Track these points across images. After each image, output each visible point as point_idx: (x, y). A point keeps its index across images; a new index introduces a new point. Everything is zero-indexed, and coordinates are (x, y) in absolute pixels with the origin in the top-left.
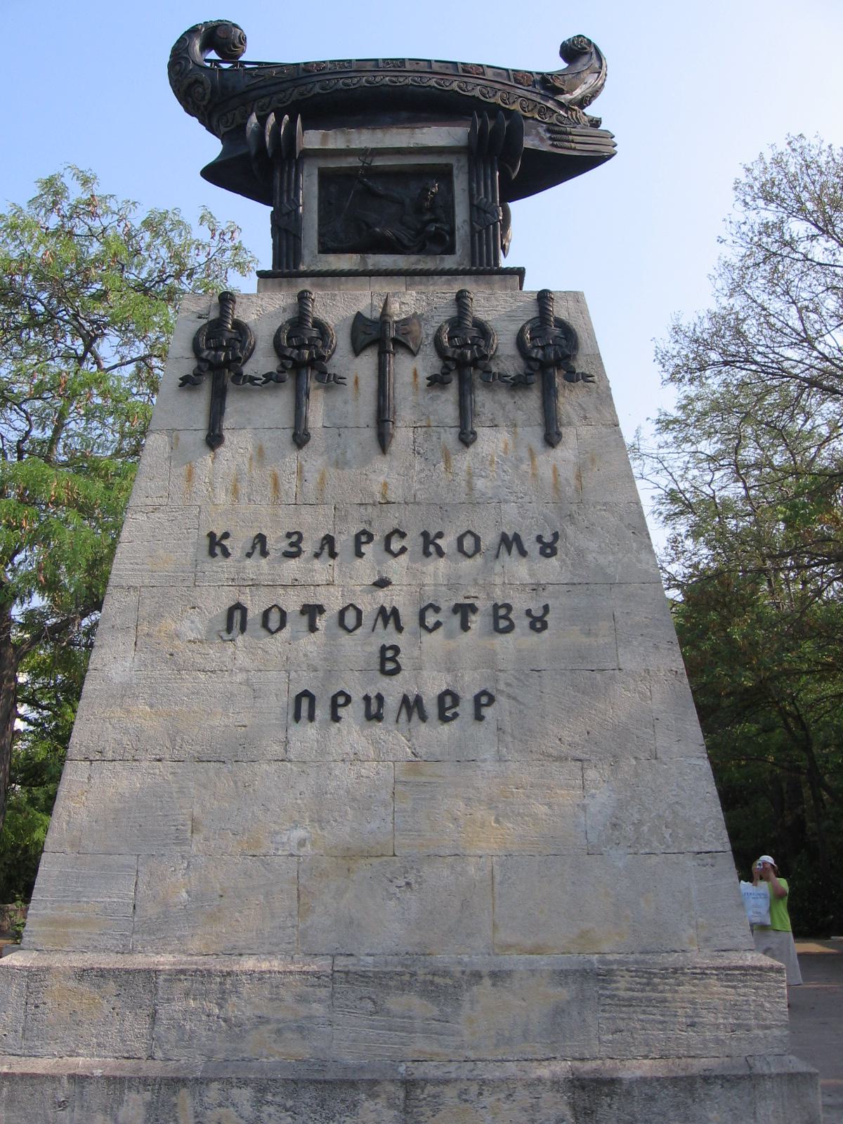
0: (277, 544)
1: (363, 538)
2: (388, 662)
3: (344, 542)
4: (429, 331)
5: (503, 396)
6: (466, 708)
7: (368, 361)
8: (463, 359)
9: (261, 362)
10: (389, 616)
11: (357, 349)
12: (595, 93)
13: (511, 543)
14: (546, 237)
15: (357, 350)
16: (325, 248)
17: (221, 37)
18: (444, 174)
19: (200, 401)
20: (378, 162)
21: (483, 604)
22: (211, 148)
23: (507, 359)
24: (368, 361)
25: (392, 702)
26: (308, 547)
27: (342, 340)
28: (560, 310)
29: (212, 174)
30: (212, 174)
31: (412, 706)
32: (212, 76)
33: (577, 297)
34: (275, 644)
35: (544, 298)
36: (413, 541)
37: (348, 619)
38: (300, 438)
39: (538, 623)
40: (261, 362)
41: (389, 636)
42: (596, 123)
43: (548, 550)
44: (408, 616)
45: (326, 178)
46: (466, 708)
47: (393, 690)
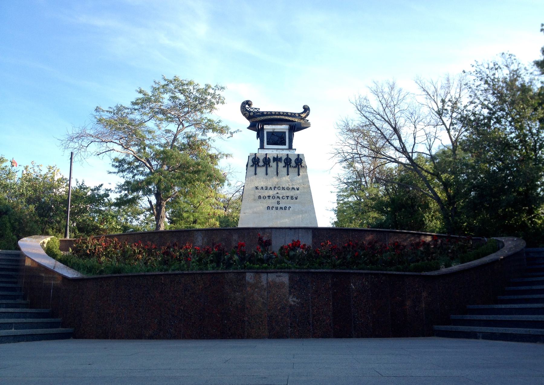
0: (264, 188)
1: (275, 188)
2: (278, 203)
3: (273, 189)
4: (283, 159)
5: (292, 169)
6: (288, 208)
7: (275, 163)
8: (288, 161)
9: (261, 163)
10: (278, 197)
11: (274, 161)
12: (308, 115)
13: (293, 188)
14: (300, 139)
15: (274, 161)
16: (267, 144)
17: (248, 103)
18: (285, 133)
19: (253, 168)
20: (276, 130)
21: (290, 196)
22: (248, 123)
23: (293, 163)
24: (275, 163)
25: (279, 208)
26: (268, 188)
27: (272, 159)
28: (300, 157)
29: (248, 128)
30: (248, 128)
31: (281, 208)
32: (246, 108)
33: (303, 155)
34: (265, 201)
35: (298, 155)
36: (281, 188)
37: (274, 197)
38: (267, 174)
39: (296, 199)
40: (261, 163)
41: (279, 200)
42: (308, 121)
43: (298, 189)
44: (281, 198)
45: (267, 132)
46: (288, 208)
47: (279, 206)
